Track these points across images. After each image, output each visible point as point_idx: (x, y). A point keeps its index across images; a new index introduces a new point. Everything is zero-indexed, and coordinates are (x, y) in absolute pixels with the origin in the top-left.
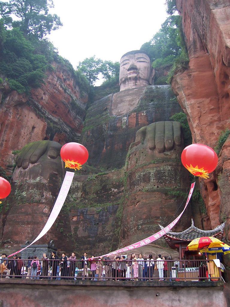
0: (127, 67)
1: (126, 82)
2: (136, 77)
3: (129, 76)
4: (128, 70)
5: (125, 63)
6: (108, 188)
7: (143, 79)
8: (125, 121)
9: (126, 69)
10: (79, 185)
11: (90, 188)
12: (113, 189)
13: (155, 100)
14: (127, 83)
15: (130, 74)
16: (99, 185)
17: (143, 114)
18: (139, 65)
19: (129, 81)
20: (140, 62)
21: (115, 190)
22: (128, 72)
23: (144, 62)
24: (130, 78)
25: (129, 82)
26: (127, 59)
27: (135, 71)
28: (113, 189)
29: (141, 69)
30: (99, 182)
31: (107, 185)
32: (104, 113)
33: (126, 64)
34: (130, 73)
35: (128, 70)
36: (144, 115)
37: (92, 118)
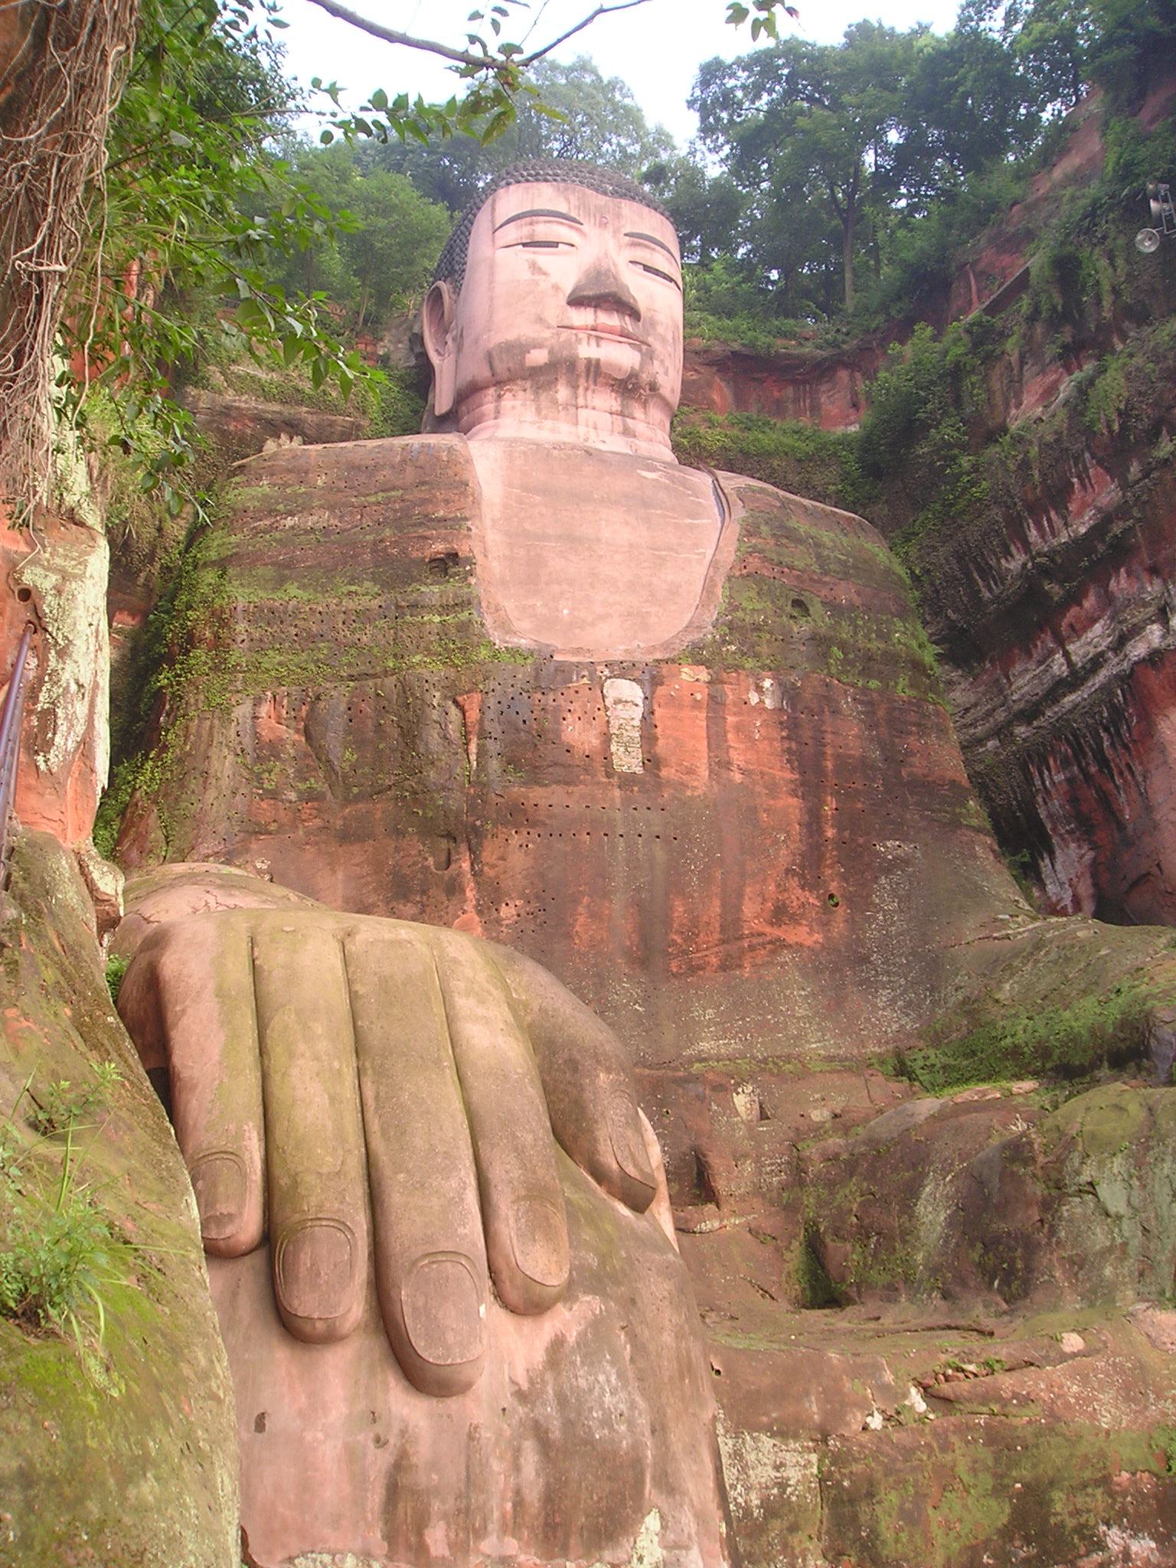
0: (565, 270)
1: (552, 383)
2: (633, 375)
3: (587, 351)
4: (577, 301)
5: (544, 230)
6: (1071, 1523)
7: (666, 404)
8: (638, 713)
9: (556, 288)
10: (793, 1475)
11: (912, 1518)
12: (1115, 1538)
13: (816, 608)
14: (563, 393)
15: (596, 332)
16: (987, 1481)
17: (754, 698)
18: (643, 290)
19: (582, 382)
20: (647, 268)
21: (1135, 1547)
22: (584, 317)
23: (671, 280)
24: (595, 371)
25: (581, 391)
26: (562, 208)
27: (628, 323)
28: (1115, 1538)
29: (660, 330)
30: (986, 1455)
31: (1052, 1483)
32: (432, 591)
33: (555, 245)
35: (577, 301)
36: (760, 708)
37: (293, 589)
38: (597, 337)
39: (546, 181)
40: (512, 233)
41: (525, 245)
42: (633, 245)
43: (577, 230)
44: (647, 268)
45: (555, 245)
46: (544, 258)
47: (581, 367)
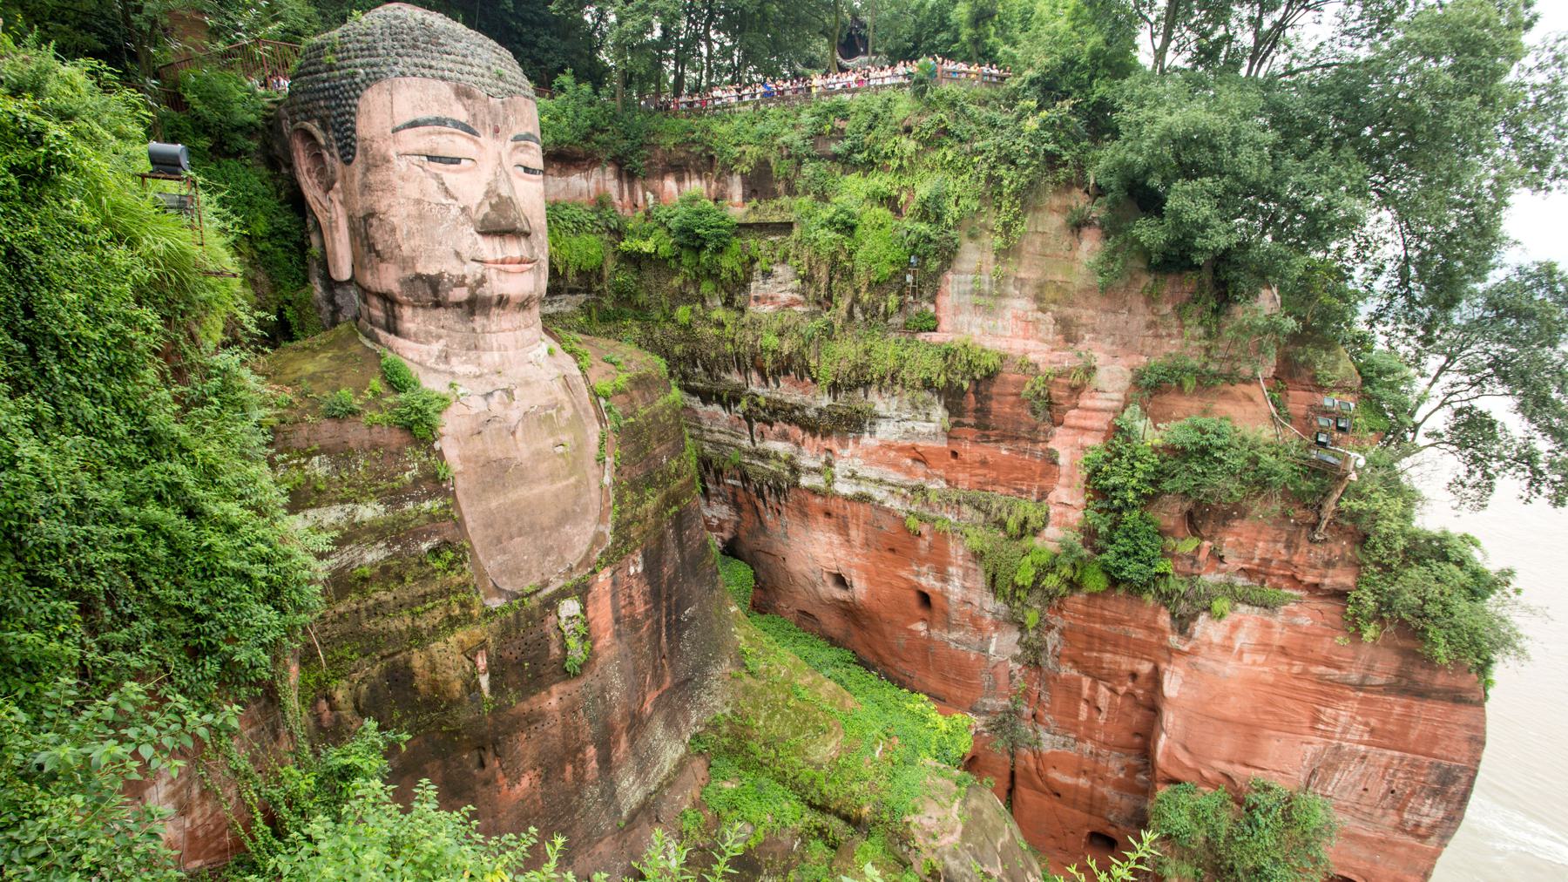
0: (470, 186)
20: (527, 170)
22: (490, 248)
24: (503, 301)
26: (460, 113)
33: (456, 161)
34: (503, 262)
38: (507, 272)
39: (443, 78)
40: (415, 140)
41: (431, 158)
42: (516, 148)
43: (476, 142)
44: (527, 170)
45: (456, 161)
46: (450, 175)
47: (495, 300)
